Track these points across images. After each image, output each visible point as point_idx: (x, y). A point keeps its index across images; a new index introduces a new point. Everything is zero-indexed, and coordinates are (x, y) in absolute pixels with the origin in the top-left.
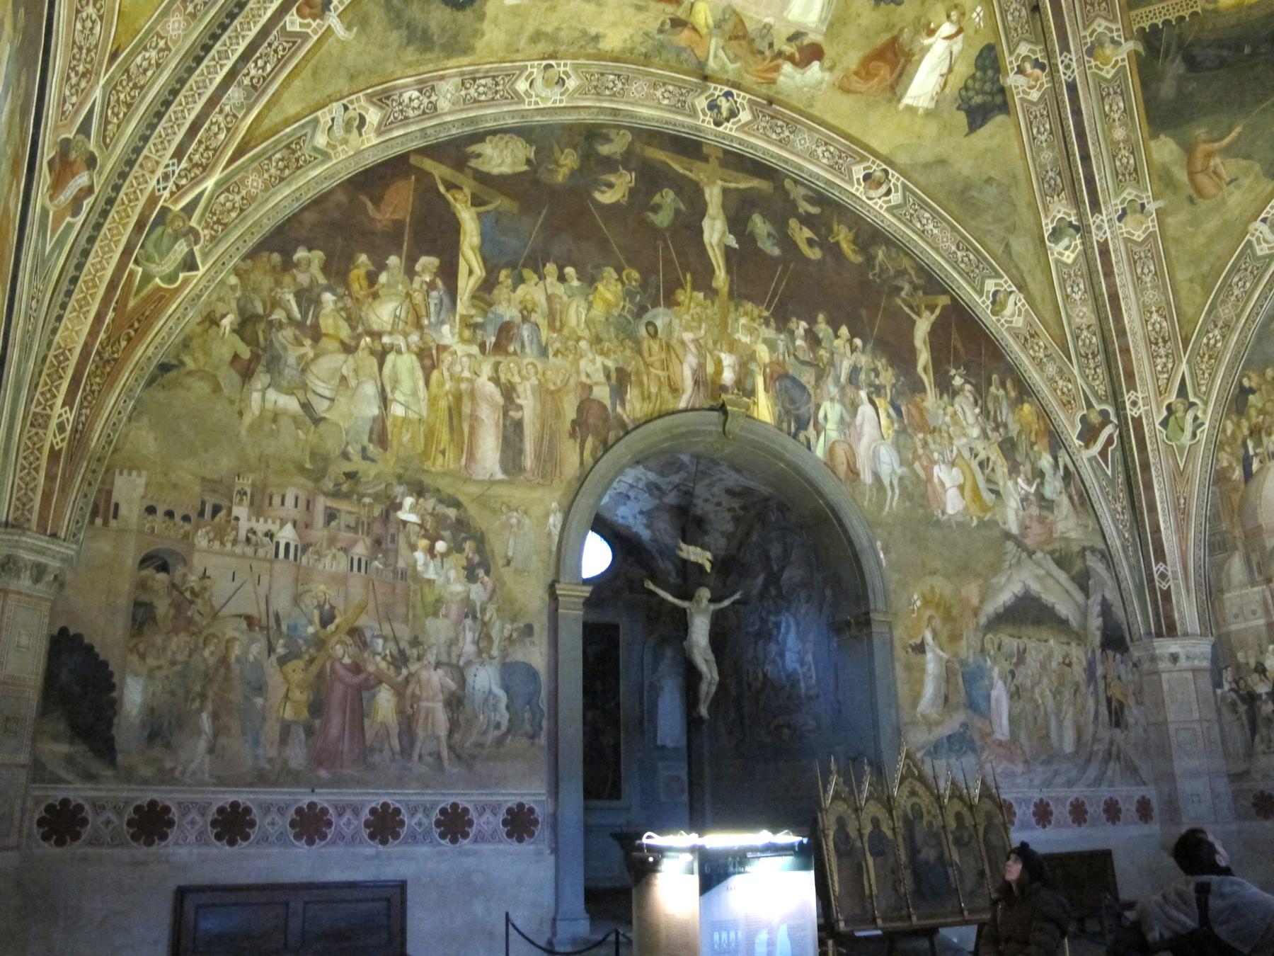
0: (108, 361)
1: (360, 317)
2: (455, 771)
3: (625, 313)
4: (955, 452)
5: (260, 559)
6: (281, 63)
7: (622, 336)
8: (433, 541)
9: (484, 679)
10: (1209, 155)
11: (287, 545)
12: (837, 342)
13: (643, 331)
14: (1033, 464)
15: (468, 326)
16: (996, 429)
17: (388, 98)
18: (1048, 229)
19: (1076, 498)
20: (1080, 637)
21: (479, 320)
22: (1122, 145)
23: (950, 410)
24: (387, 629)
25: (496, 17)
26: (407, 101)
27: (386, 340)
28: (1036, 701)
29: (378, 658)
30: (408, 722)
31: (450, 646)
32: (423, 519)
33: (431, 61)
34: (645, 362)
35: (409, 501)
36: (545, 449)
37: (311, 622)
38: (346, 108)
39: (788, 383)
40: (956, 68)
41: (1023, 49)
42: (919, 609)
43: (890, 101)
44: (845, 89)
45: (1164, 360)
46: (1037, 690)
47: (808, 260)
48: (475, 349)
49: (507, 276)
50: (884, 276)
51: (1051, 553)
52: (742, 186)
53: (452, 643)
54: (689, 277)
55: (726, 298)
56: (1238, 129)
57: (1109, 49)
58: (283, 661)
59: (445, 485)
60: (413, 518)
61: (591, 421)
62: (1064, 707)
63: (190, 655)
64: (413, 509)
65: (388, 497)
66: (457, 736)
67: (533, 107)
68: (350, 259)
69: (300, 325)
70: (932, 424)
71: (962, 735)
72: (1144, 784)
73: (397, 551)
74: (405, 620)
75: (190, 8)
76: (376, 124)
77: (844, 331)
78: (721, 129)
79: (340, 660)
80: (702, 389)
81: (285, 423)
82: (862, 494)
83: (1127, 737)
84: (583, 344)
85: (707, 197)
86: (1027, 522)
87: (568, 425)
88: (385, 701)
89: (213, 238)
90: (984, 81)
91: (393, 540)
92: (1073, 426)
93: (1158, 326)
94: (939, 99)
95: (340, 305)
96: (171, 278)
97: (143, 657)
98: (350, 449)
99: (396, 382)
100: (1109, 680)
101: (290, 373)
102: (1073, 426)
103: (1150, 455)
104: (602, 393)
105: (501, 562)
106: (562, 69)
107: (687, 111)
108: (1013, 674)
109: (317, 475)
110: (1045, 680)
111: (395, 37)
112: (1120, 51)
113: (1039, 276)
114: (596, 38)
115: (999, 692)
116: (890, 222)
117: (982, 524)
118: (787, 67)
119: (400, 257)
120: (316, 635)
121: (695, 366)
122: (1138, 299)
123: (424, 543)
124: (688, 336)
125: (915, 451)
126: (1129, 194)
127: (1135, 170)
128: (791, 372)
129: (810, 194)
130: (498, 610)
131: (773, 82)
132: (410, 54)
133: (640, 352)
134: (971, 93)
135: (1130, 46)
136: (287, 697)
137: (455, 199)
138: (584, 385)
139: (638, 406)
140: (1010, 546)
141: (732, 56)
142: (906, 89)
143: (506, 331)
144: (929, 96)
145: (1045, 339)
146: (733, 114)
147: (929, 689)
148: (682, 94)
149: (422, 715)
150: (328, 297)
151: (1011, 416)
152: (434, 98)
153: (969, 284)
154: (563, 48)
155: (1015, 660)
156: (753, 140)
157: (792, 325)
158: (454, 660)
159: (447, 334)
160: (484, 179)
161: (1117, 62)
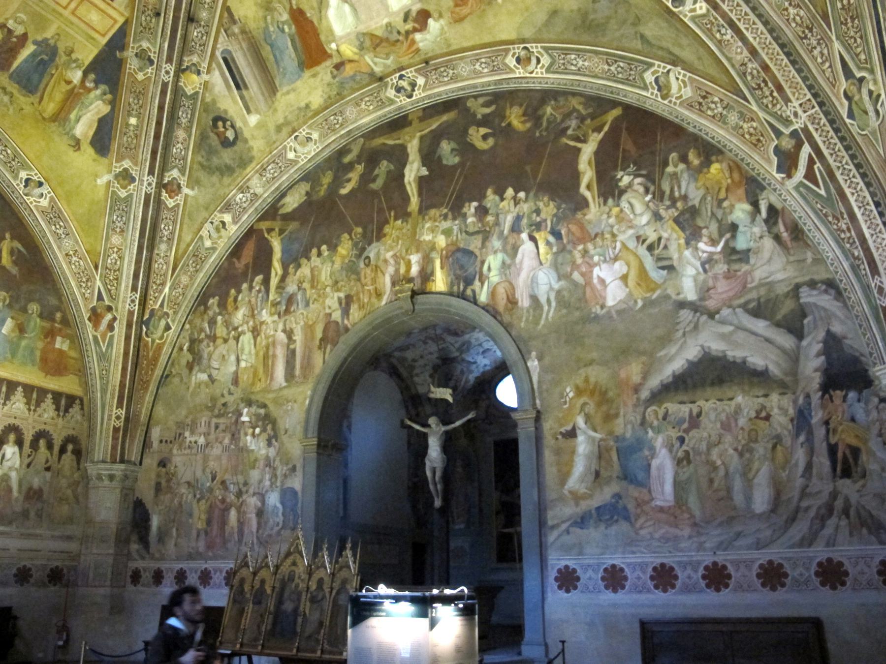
4: (618, 245)
6: (174, 222)
8: (254, 428)
9: (273, 499)
13: (362, 265)
14: (719, 222)
20: (784, 387)
23: (616, 210)
24: (235, 480)
25: (253, 135)
28: (714, 463)
30: (241, 523)
32: (251, 418)
33: (238, 176)
35: (246, 410)
36: (306, 361)
38: (212, 223)
39: (459, 255)
42: (571, 399)
44: (459, 20)
45: (819, 49)
46: (715, 452)
47: (484, 152)
48: (276, 317)
51: (744, 306)
52: (434, 127)
53: (260, 481)
54: (392, 214)
58: (199, 500)
62: (756, 465)
66: (260, 532)
68: (227, 294)
73: (240, 438)
78: (414, 98)
81: (203, 386)
82: (520, 319)
83: (864, 486)
84: (328, 289)
85: (409, 150)
86: (711, 283)
87: (317, 342)
88: (233, 514)
91: (239, 433)
92: (769, 161)
96: (161, 338)
99: (243, 350)
100: (831, 426)
101: (205, 362)
102: (769, 161)
104: (337, 316)
105: (282, 432)
107: (387, 103)
108: (682, 440)
109: (211, 409)
110: (728, 439)
111: (215, 179)
113: (685, 41)
114: (307, 106)
116: (555, 80)
117: (649, 303)
118: (418, 36)
123: (251, 431)
125: (574, 263)
128: (462, 246)
130: (281, 460)
131: (418, 50)
132: (226, 180)
133: (359, 280)
140: (686, 315)
143: (291, 300)
145: (719, 93)
146: (413, 85)
147: (579, 467)
148: (376, 97)
150: (219, 318)
151: (692, 186)
152: (252, 191)
153: (632, 86)
155: (685, 426)
157: (465, 210)
159: (265, 315)
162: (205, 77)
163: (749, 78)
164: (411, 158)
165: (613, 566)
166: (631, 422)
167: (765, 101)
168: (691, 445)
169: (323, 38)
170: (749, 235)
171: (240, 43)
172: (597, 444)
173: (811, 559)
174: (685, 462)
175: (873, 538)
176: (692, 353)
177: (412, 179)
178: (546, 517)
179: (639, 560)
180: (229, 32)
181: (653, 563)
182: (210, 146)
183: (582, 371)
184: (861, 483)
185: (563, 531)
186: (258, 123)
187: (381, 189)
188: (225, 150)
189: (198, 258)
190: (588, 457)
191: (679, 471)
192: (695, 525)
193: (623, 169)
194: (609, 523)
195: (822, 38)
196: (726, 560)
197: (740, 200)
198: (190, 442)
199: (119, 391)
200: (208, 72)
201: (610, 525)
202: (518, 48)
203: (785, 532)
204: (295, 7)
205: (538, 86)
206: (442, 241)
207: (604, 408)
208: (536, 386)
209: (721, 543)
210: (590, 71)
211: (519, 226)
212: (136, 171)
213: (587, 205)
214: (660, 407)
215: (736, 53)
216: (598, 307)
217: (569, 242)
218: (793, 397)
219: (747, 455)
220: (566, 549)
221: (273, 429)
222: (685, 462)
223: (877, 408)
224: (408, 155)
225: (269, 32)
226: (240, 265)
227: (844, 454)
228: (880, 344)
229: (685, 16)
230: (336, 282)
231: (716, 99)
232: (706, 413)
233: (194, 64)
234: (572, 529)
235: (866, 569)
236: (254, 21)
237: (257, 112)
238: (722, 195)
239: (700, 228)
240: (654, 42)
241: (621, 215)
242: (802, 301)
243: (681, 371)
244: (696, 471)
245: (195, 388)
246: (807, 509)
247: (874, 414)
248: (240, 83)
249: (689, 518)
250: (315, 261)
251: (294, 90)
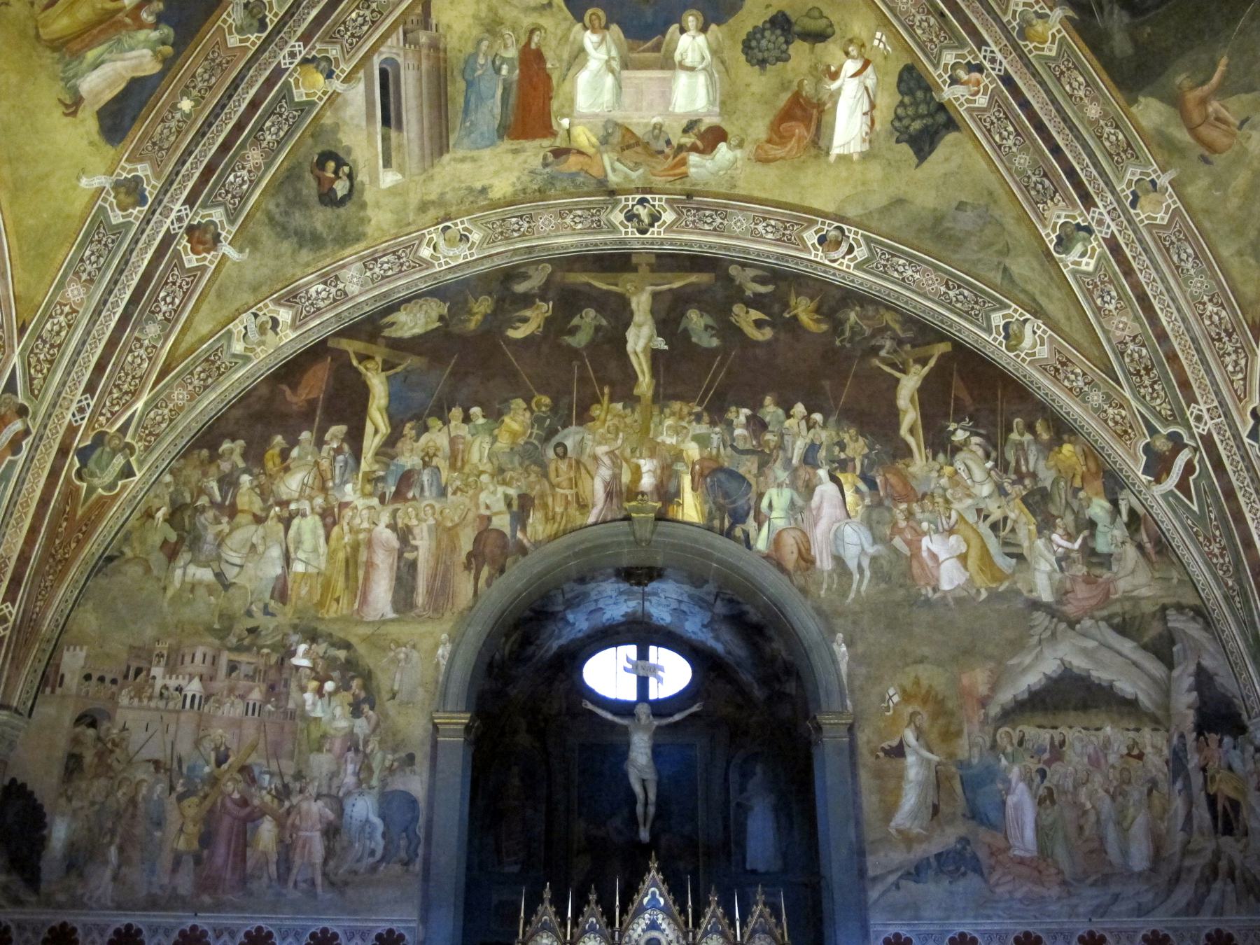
0: (60, 561)
1: (272, 491)
2: (329, 896)
3: (533, 440)
4: (954, 515)
5: (170, 711)
6: (187, 295)
7: (527, 463)
8: (322, 681)
9: (363, 808)
10: (1203, 102)
11: (194, 697)
12: (788, 423)
13: (551, 453)
15: (369, 481)
16: (1020, 478)
17: (295, 297)
18: (1051, 240)
19: (1148, 546)
20: (1157, 723)
21: (382, 473)
22: (1102, 123)
24: (274, 766)
26: (314, 295)
27: (293, 506)
28: (1083, 805)
29: (264, 792)
30: (286, 849)
31: (331, 779)
32: (315, 663)
33: (327, 256)
34: (551, 483)
35: (303, 648)
36: (438, 583)
37: (208, 763)
38: (256, 315)
39: (722, 476)
40: (878, 102)
41: (949, 58)
42: (896, 705)
43: (816, 157)
44: (765, 161)
45: (1234, 357)
46: (1083, 792)
47: (756, 344)
48: (375, 501)
49: (412, 429)
50: (858, 338)
51: (1108, 619)
52: (676, 285)
53: (333, 775)
54: (606, 390)
55: (649, 402)
56: (1224, 61)
57: (1039, 26)
58: (181, 798)
59: (338, 632)
60: (305, 663)
61: (487, 551)
62: (1131, 811)
63: (107, 797)
64: (306, 654)
65: (284, 646)
66: (332, 863)
67: (444, 267)
68: (266, 441)
69: (219, 506)
70: (920, 490)
73: (288, 694)
74: (292, 758)
75: (84, 277)
76: (289, 322)
77: (799, 409)
78: (647, 235)
79: (230, 795)
80: (615, 500)
81: (201, 591)
84: (485, 478)
85: (634, 306)
86: (1068, 585)
88: (267, 831)
89: (146, 448)
90: (915, 104)
91: (286, 685)
92: (1135, 457)
93: (1216, 318)
94: (871, 137)
95: (255, 483)
96: (111, 486)
97: (69, 799)
98: (254, 608)
99: (299, 543)
100: (1209, 774)
101: (208, 548)
102: (1135, 457)
103: (1233, 478)
104: (502, 522)
106: (460, 227)
108: (1043, 774)
109: (222, 634)
110: (1098, 778)
111: (286, 247)
112: (1051, 22)
113: (1056, 293)
114: (484, 190)
115: (1022, 803)
116: (864, 280)
117: (994, 596)
118: (694, 158)
119: (311, 431)
120: (210, 774)
121: (608, 478)
122: (1184, 292)
124: (601, 450)
125: (895, 524)
126: (1133, 174)
127: (1129, 145)
128: (726, 464)
129: (760, 273)
130: (380, 742)
131: (685, 175)
132: (305, 255)
133: (545, 475)
134: (906, 122)
135: (1058, 13)
136: (181, 830)
137: (367, 369)
138: (481, 517)
139: (540, 528)
140: (1040, 618)
141: (632, 165)
142: (831, 140)
143: (406, 479)
144: (859, 139)
145: (1081, 364)
146: (655, 218)
147: (910, 799)
148: (593, 215)
149: (300, 842)
150: (245, 479)
151: (1042, 464)
152: (341, 286)
153: (971, 322)
154: (454, 208)
155: (1046, 756)
156: (685, 237)
157: (731, 415)
158: (334, 792)
159: (349, 492)
160: (399, 345)
161: (1054, 36)
162: (337, 85)
163: (1127, 360)
164: (637, 318)
165: (962, 935)
166: (977, 744)
167: (1142, 390)
169: (555, 105)
170: (1109, 537)
171: (420, 61)
176: (1050, 666)
177: (639, 349)
180: (410, 36)
182: (298, 193)
183: (912, 671)
186: (394, 187)
187: (587, 347)
188: (322, 208)
189: (214, 367)
190: (923, 785)
193: (958, 423)
195: (1242, 348)
197: (1097, 494)
198: (166, 687)
199: (16, 568)
200: (347, 80)
202: (829, 225)
204: (533, 46)
205: (838, 280)
206: (693, 451)
207: (941, 721)
208: (845, 680)
209: (1098, 906)
210: (918, 286)
211: (815, 458)
212: (154, 187)
213: (908, 452)
214: (1014, 729)
215: (1117, 328)
216: (929, 589)
217: (887, 496)
219: (1120, 799)
220: (895, 911)
221: (365, 687)
224: (632, 314)
225: (476, 62)
226: (296, 399)
229: (1066, 266)
230: (501, 471)
231: (1078, 370)
233: (328, 59)
234: (903, 883)
236: (460, 38)
237: (401, 170)
238: (1078, 483)
239: (1055, 517)
240: (1018, 281)
241: (956, 478)
242: (1170, 625)
243: (1038, 687)
245: (182, 589)
248: (393, 115)
250: (456, 425)
251: (473, 160)
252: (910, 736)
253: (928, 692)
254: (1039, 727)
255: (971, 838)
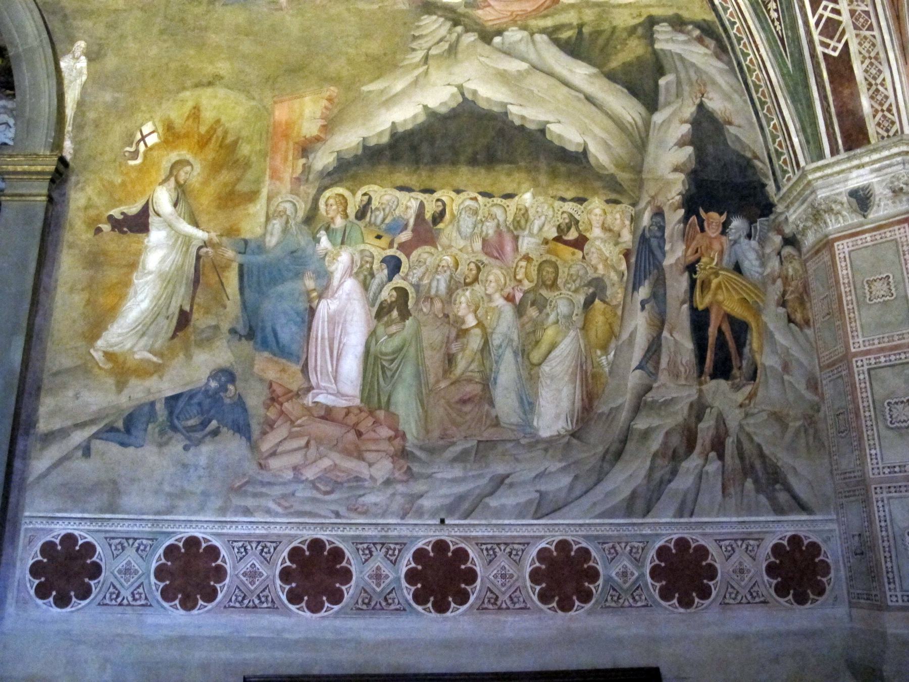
42: (149, 149)
46: (464, 298)
51: (552, 33)
62: (550, 333)
71: (214, 397)
72: (803, 508)
83: (751, 396)
100: (699, 276)
108: (394, 266)
110: (495, 275)
155: (405, 236)
165: (192, 542)
166: (281, 214)
168: (414, 280)
172: (193, 251)
173: (646, 540)
174: (395, 313)
175: (763, 499)
178: (35, 410)
179: (260, 531)
181: (294, 537)
184: (748, 389)
185: (77, 448)
190: (168, 280)
191: (381, 330)
192: (403, 454)
194: (199, 435)
196: (466, 539)
201: (199, 442)
203: (599, 481)
207: (225, 176)
209: (461, 498)
214: (354, 193)
218: (631, 210)
219: (533, 312)
222: (395, 313)
223: (779, 254)
227: (720, 330)
228: (795, 140)
232: (453, 216)
234: (97, 445)
235: (748, 563)
242: (657, 46)
243: (409, 126)
244: (417, 335)
246: (646, 435)
247: (774, 264)
249: (390, 439)
252: (163, 199)
253: (212, 130)
254: (401, 188)
255: (238, 371)
